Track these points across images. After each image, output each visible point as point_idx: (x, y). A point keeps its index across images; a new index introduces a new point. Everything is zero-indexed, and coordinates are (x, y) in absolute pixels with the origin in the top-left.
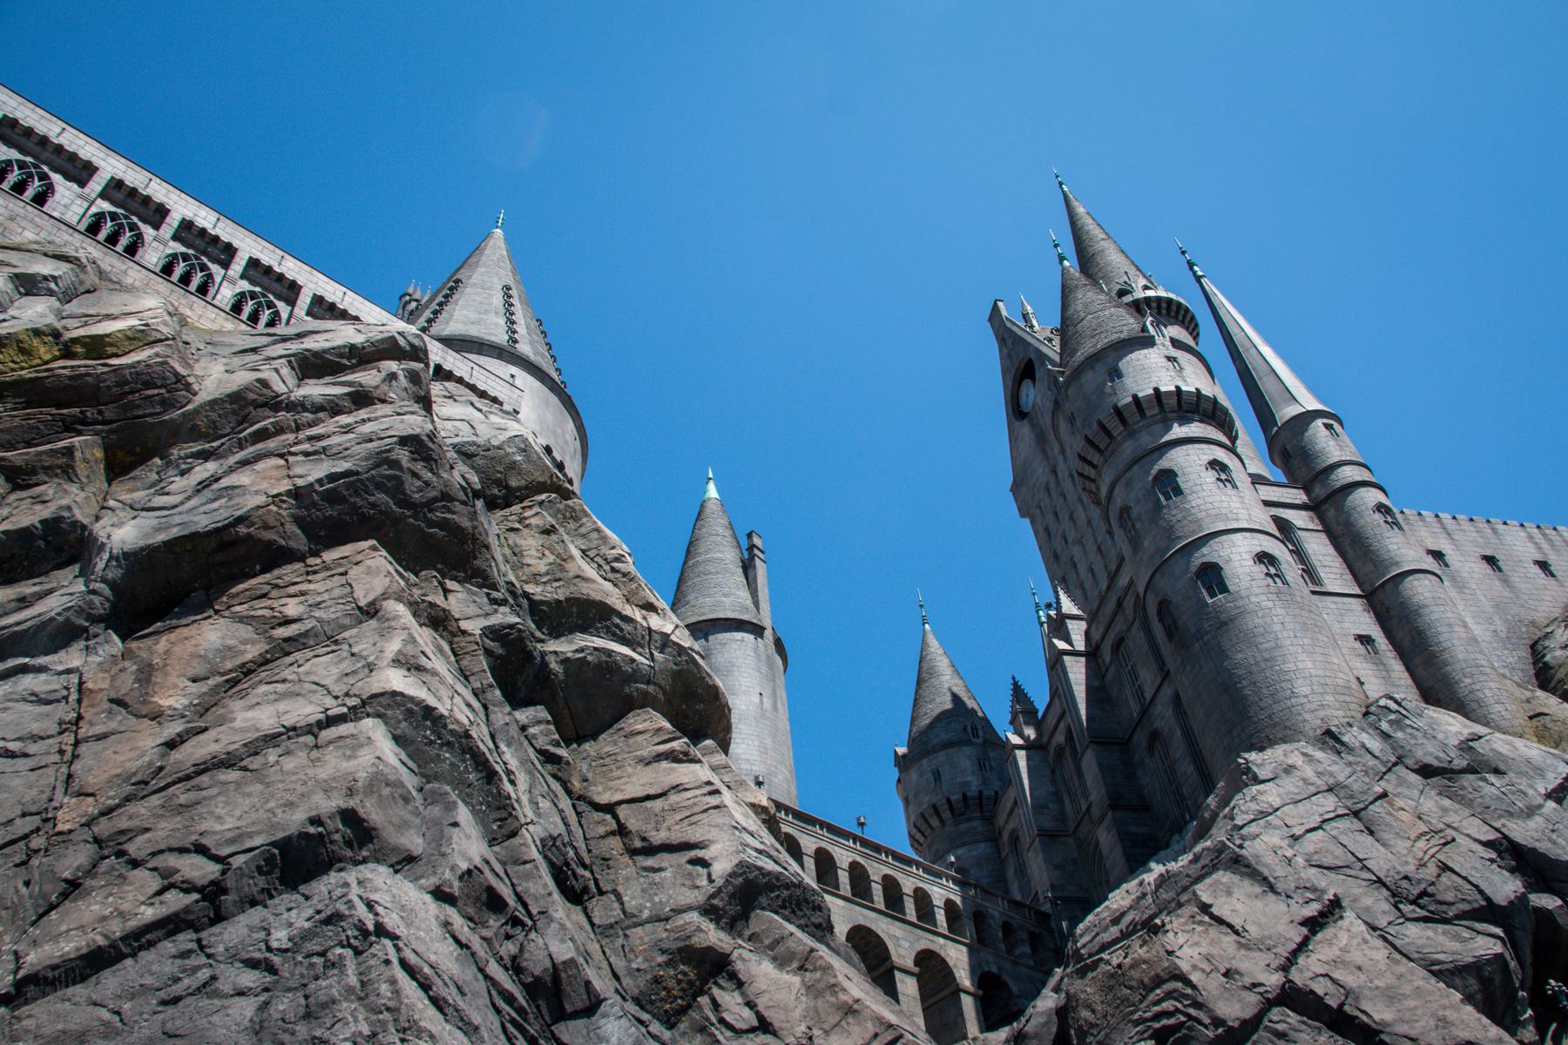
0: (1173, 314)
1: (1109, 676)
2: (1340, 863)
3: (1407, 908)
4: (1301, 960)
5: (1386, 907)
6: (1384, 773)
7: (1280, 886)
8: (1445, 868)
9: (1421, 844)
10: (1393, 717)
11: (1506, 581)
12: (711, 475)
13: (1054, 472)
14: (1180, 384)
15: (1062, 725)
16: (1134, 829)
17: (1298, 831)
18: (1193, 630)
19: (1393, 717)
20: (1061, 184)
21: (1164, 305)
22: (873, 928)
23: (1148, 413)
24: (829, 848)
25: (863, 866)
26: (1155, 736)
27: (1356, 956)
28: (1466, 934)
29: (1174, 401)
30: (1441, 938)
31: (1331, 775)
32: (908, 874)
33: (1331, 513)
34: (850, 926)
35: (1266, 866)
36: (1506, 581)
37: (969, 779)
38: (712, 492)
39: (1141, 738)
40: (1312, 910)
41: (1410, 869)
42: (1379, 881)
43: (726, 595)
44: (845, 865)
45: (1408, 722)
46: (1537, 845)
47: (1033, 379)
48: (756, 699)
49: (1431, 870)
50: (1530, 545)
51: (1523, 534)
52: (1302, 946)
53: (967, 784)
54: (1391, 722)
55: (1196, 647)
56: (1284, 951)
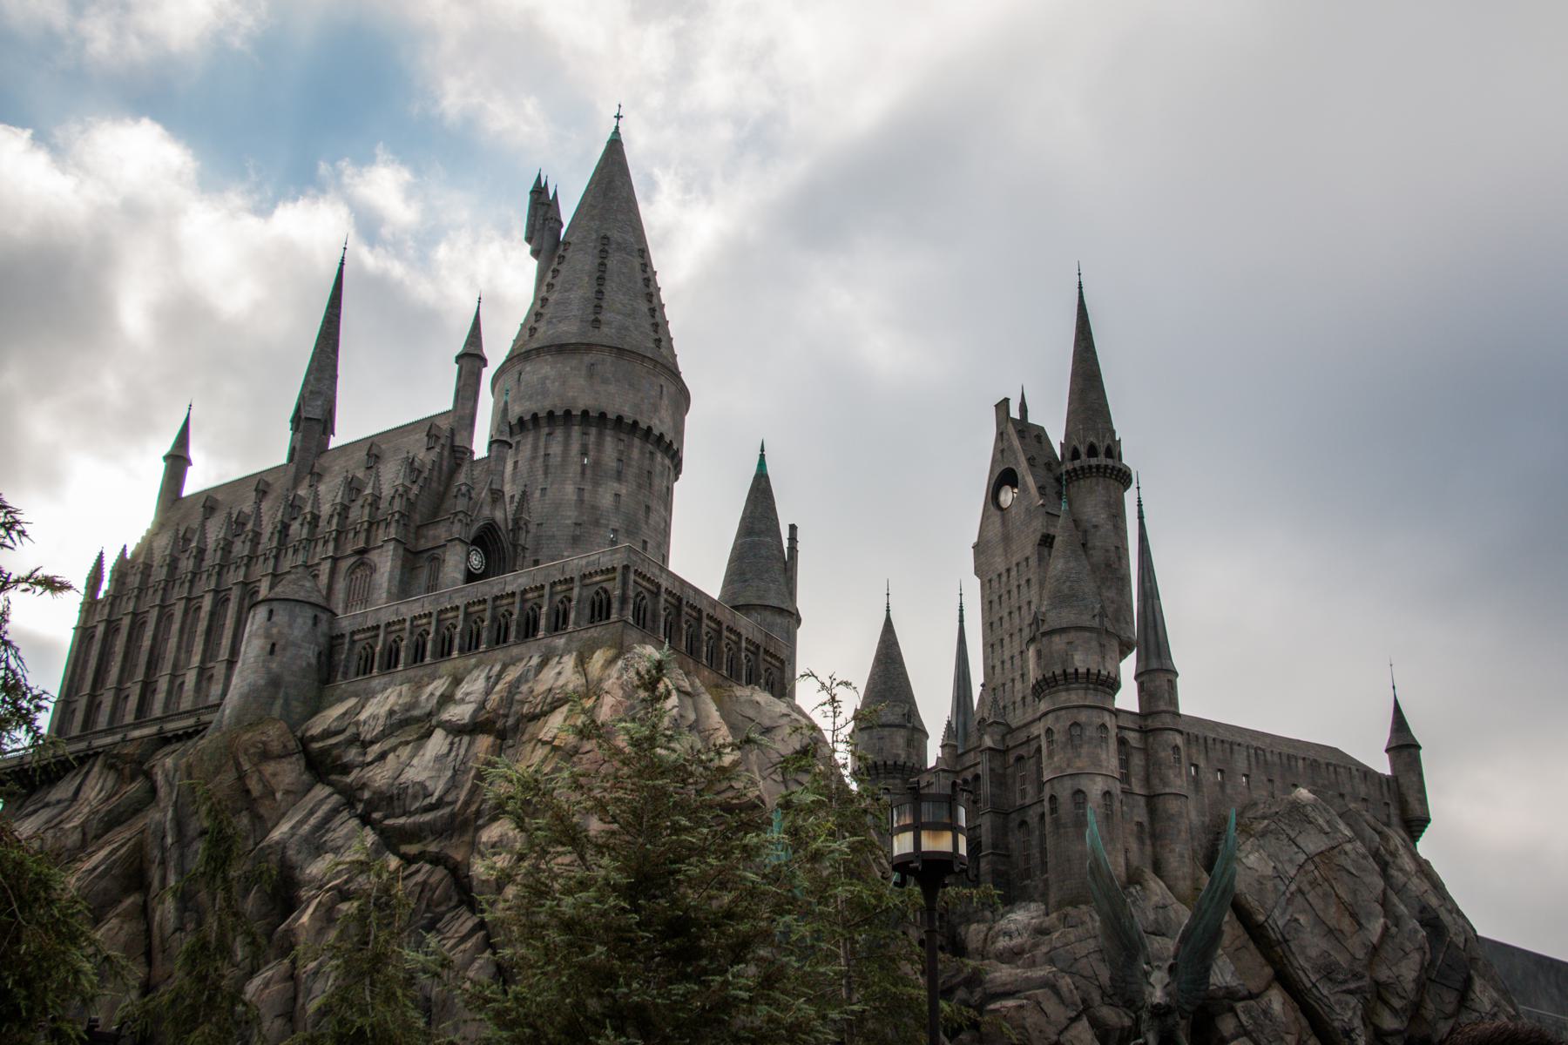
1: (1009, 771)
3: (1105, 999)
4: (1065, 1033)
5: (1099, 998)
13: (1008, 570)
14: (1101, 668)
15: (972, 769)
16: (1000, 867)
18: (1063, 821)
26: (1023, 823)
27: (1082, 1036)
28: (1122, 1014)
30: (1114, 1015)
33: (1151, 739)
36: (1222, 785)
37: (900, 752)
39: (1015, 819)
40: (1073, 1014)
43: (773, 582)
47: (1014, 484)
50: (1246, 762)
52: (1066, 1028)
53: (898, 755)
55: (1062, 831)
56: (1060, 1028)
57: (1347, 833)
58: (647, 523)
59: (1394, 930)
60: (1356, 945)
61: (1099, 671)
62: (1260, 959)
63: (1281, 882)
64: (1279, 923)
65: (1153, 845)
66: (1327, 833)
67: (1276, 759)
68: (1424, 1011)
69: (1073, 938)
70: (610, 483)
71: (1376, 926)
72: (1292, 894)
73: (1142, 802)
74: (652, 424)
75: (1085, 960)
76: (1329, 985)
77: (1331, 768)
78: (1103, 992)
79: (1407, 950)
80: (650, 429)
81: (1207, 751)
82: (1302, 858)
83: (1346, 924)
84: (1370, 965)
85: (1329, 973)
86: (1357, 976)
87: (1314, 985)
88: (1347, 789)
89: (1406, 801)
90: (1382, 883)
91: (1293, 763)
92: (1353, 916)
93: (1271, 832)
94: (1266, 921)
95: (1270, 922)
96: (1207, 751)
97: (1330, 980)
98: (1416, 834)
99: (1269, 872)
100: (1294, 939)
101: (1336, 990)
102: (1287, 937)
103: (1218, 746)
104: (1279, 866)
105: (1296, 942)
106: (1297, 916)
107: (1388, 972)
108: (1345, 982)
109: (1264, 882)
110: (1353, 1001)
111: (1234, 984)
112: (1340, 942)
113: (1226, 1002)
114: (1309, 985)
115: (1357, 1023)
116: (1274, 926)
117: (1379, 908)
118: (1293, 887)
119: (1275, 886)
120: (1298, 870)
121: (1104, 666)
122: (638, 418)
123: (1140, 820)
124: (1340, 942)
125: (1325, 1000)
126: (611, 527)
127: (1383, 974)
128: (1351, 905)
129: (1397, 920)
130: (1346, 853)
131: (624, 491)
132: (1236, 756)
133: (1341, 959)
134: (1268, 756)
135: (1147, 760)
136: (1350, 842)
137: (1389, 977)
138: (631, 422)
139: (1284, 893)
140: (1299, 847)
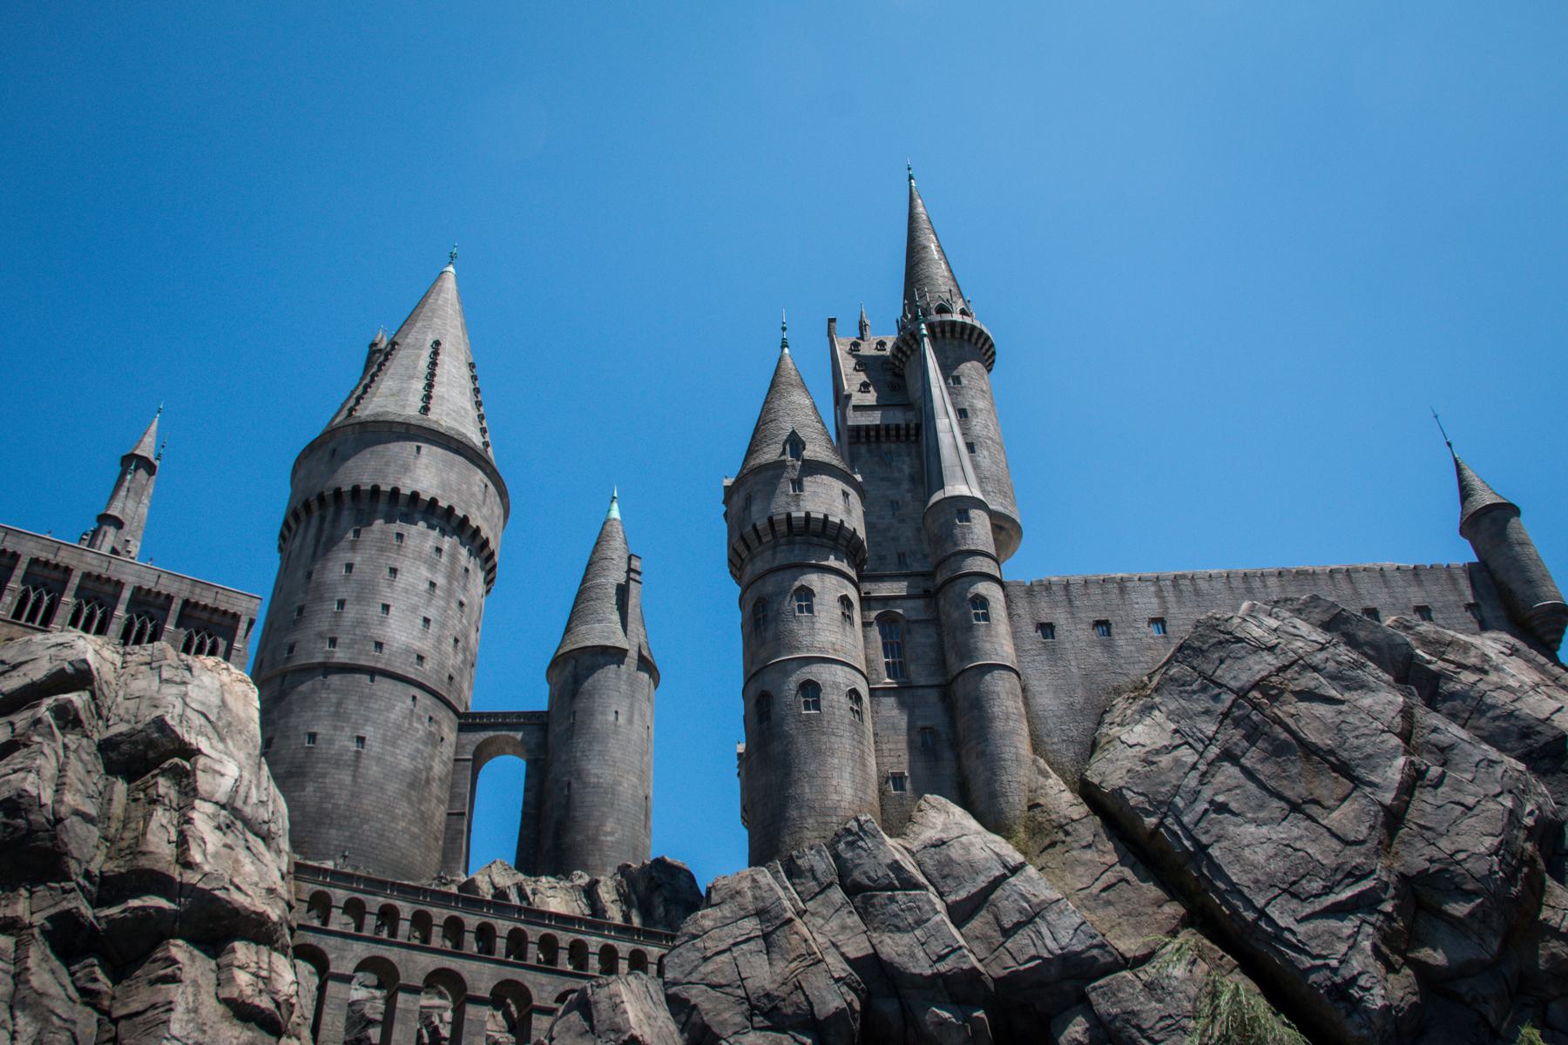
0: (957, 335)
2: (723, 982)
5: (739, 1019)
6: (817, 894)
7: (599, 1027)
8: (799, 987)
9: (793, 965)
10: (850, 839)
11: (1109, 648)
12: (616, 495)
17: (709, 954)
19: (850, 839)
20: (911, 178)
21: (948, 329)
22: (520, 980)
23: (764, 540)
24: (492, 921)
25: (523, 931)
29: (784, 528)
31: (763, 899)
32: (567, 930)
34: (496, 983)
35: (598, 1011)
36: (1109, 648)
38: (615, 513)
41: (769, 987)
42: (748, 998)
44: (505, 933)
45: (861, 843)
46: (897, 959)
48: (612, 718)
49: (790, 986)
51: (1153, 589)
54: (848, 844)
57: (1314, 637)
58: (390, 586)
59: (1435, 771)
60: (1349, 816)
61: (789, 515)
62: (1152, 891)
63: (1191, 751)
64: (1186, 819)
65: (958, 758)
66: (1271, 649)
67: (1218, 585)
68: (1545, 913)
69: (708, 923)
70: (341, 555)
71: (1394, 771)
72: (1211, 764)
73: (933, 696)
74: (399, 485)
75: (725, 957)
76: (1294, 904)
77: (1339, 576)
78: (753, 1007)
79: (1470, 801)
80: (395, 491)
81: (1070, 601)
82: (1228, 699)
83: (1327, 786)
84: (1385, 848)
85: (1295, 883)
86: (1355, 875)
87: (1262, 913)
88: (1379, 599)
89: (1510, 591)
90: (1401, 699)
91: (1257, 584)
92: (1343, 769)
93: (1171, 679)
94: (1161, 823)
95: (1169, 821)
96: (1070, 601)
97: (1295, 896)
98: (1549, 638)
99: (1164, 740)
100: (1219, 839)
101: (1308, 910)
102: (1204, 839)
103: (1095, 591)
104: (1184, 726)
105: (1225, 844)
106: (1220, 799)
107: (1429, 851)
108: (1327, 890)
109: (1156, 759)
110: (1347, 926)
111: (1079, 948)
112: (1314, 820)
113: (1068, 986)
114: (1250, 916)
115: (1362, 962)
116: (1176, 828)
117: (1395, 741)
118: (1214, 751)
119: (1177, 761)
120: (1221, 723)
121: (798, 506)
122: (379, 482)
123: (928, 724)
124: (1314, 820)
125: (1287, 935)
126: (337, 598)
127: (1416, 858)
128: (1332, 752)
129: (1444, 753)
130: (1315, 669)
131: (357, 559)
132: (1133, 596)
133: (1322, 851)
134: (1203, 585)
135: (939, 635)
136: (1323, 648)
137: (1431, 860)
138: (369, 488)
139: (1194, 767)
140: (1220, 685)
